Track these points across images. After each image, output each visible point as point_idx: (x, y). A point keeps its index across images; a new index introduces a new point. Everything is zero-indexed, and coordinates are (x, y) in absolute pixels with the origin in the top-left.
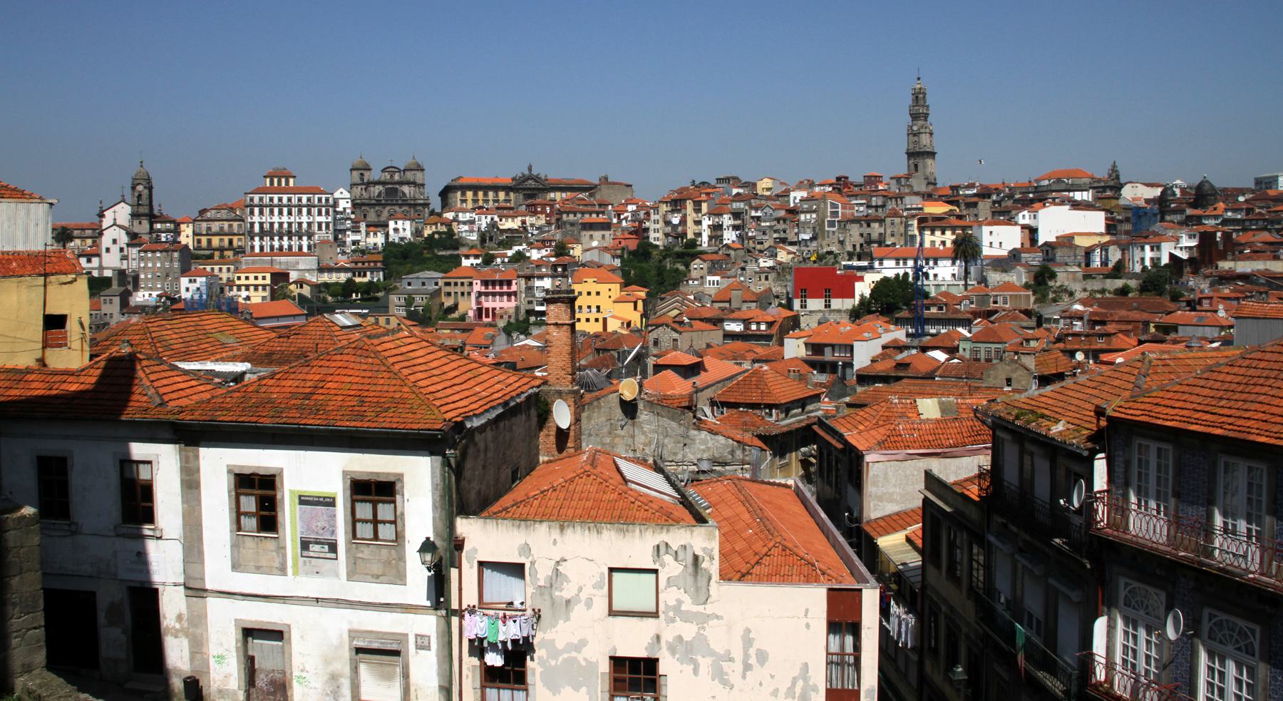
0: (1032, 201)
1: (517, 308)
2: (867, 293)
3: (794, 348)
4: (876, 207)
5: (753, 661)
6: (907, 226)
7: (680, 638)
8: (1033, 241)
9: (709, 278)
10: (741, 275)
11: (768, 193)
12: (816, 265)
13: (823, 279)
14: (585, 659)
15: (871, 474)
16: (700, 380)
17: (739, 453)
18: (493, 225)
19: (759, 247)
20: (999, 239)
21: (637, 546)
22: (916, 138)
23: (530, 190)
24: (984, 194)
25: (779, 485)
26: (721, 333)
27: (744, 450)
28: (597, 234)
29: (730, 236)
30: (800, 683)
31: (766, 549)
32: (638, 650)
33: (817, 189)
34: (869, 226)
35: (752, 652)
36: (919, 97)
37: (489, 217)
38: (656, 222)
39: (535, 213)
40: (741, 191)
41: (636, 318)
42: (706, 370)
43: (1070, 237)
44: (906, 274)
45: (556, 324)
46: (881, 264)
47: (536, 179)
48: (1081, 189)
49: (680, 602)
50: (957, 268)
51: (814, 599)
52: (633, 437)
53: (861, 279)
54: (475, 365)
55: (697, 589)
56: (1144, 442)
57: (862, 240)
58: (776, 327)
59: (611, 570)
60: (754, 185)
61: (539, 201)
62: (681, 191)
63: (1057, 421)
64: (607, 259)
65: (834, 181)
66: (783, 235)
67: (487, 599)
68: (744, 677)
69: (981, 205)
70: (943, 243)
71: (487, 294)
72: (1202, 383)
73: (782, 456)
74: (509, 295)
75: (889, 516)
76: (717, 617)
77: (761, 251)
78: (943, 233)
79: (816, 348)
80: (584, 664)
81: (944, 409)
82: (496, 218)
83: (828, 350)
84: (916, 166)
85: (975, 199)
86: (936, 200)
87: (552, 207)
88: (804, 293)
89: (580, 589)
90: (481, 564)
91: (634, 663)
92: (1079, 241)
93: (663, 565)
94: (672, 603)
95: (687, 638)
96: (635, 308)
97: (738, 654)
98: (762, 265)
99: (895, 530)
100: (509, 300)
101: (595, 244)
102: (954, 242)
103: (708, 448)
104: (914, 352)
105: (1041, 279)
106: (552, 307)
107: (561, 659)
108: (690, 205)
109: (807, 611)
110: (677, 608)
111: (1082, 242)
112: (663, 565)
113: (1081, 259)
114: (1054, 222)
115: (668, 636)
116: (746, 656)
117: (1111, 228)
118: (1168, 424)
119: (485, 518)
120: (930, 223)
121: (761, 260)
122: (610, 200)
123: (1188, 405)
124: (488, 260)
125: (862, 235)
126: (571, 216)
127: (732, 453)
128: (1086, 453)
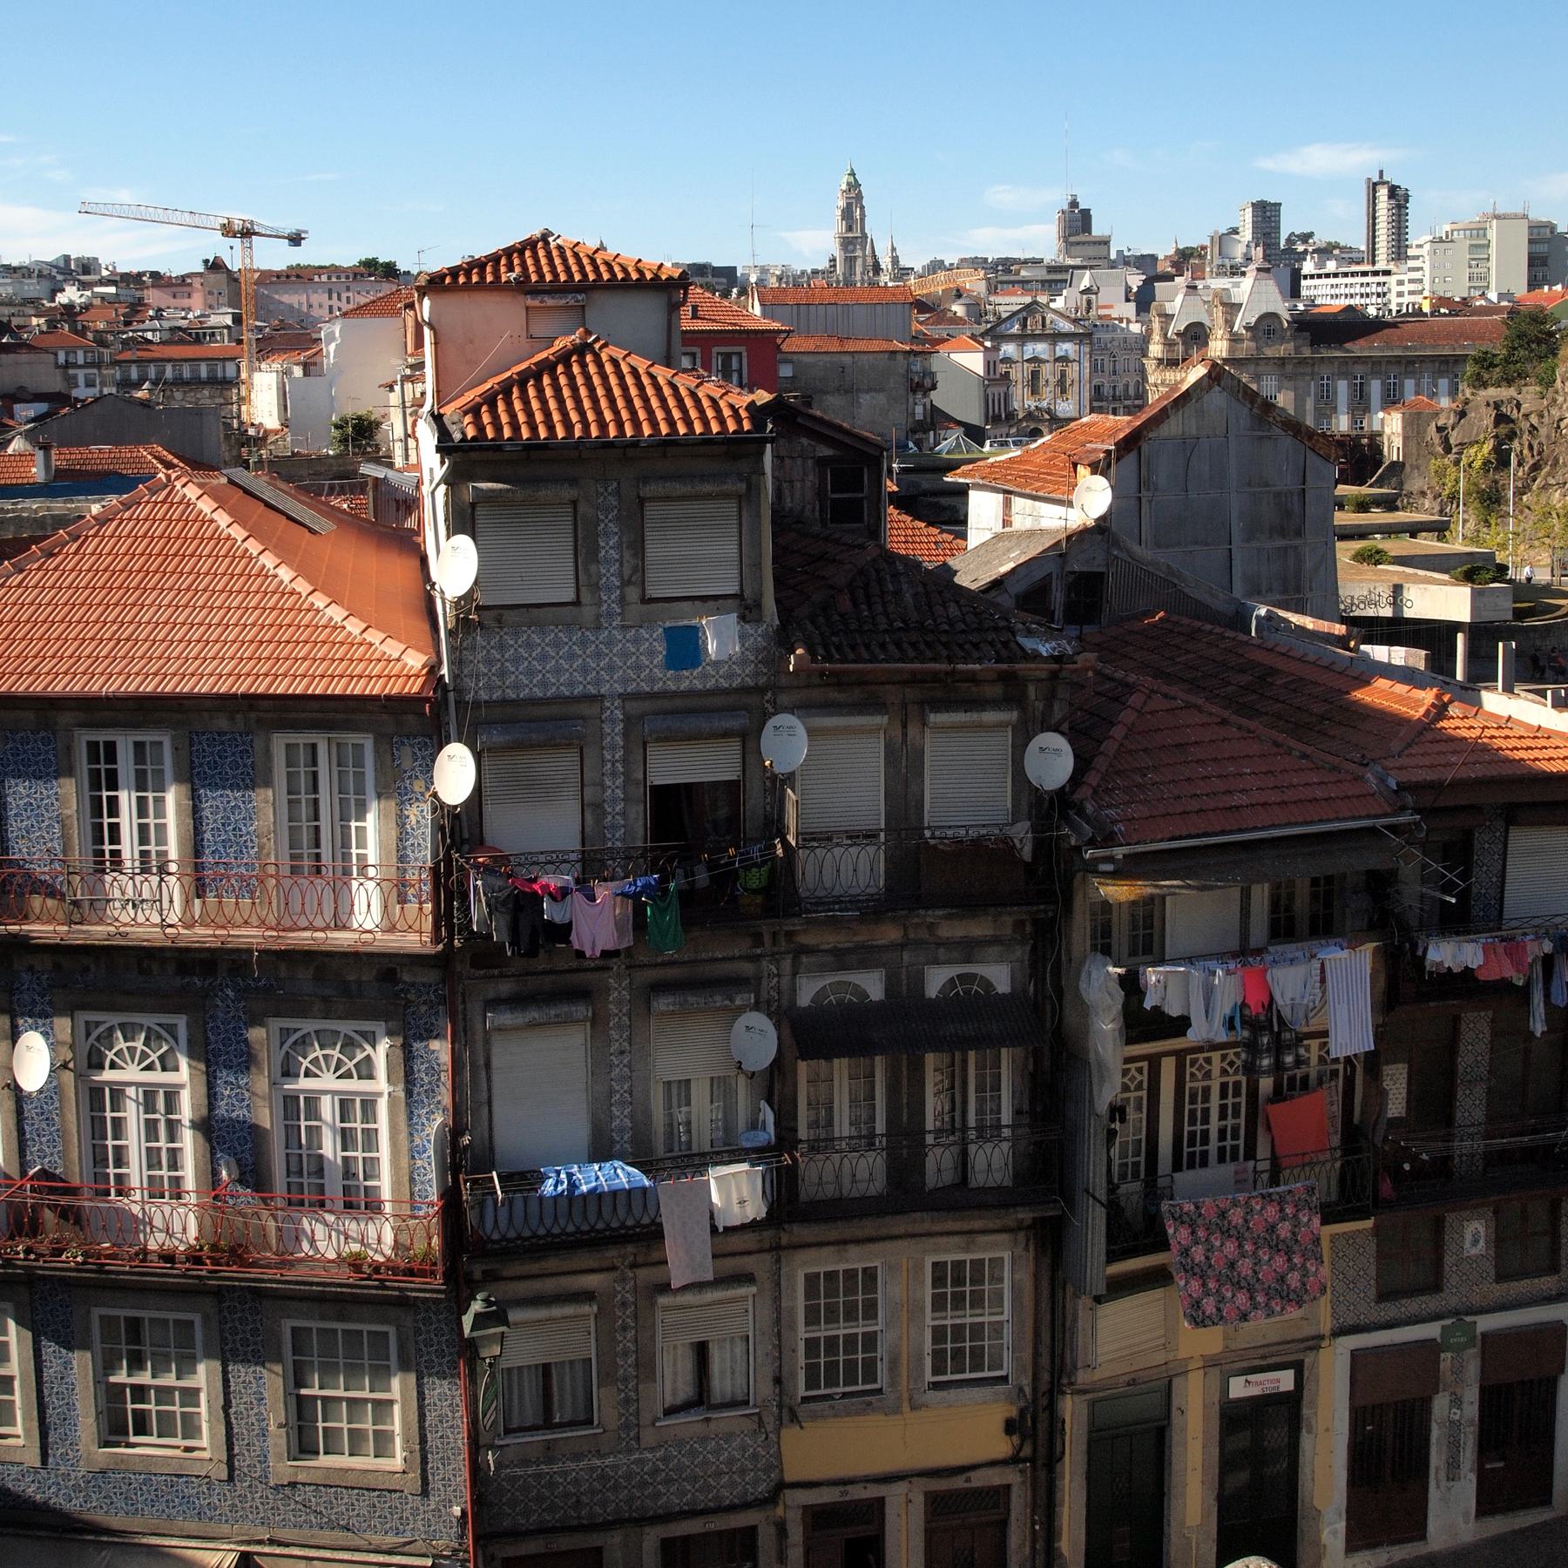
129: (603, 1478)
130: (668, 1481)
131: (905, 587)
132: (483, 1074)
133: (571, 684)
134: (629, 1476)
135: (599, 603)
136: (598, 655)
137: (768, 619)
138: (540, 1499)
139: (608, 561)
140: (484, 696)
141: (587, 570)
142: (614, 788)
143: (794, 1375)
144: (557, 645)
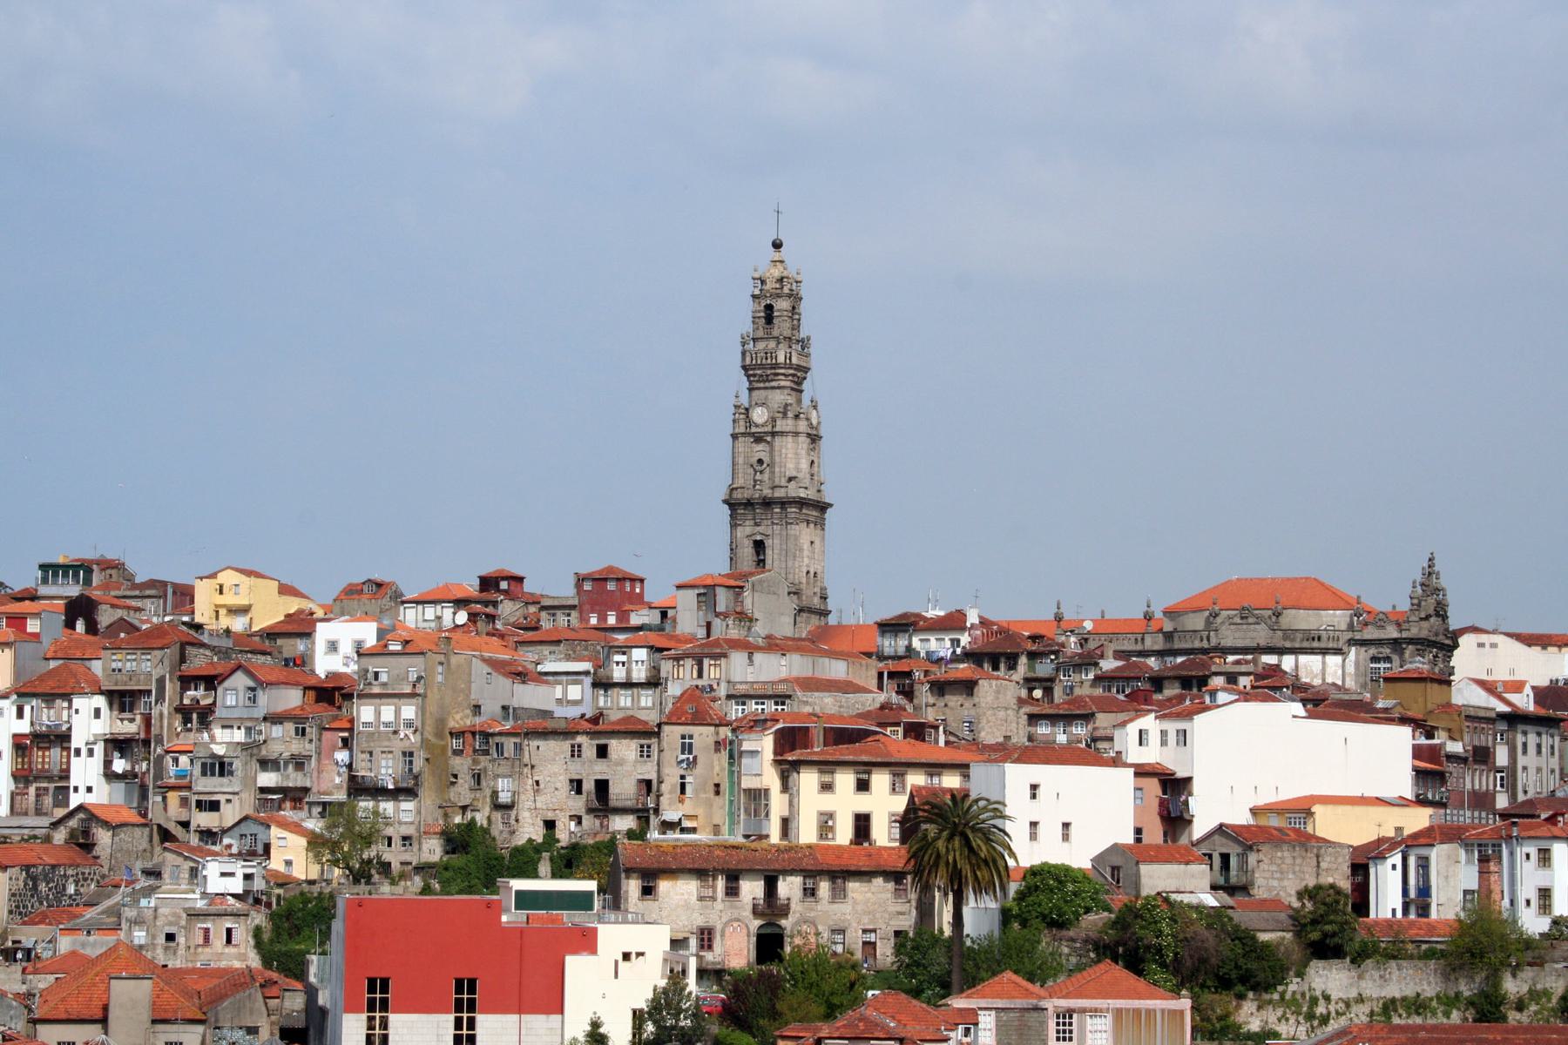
0: (1158, 682)
4: (628, 685)
6: (735, 756)
19: (204, 820)
22: (760, 451)
33: (411, 617)
34: (602, 752)
36: (775, 308)
43: (1303, 809)
48: (1314, 644)
53: (586, 942)
65: (471, 587)
66: (294, 779)
69: (987, 690)
77: (208, 835)
78: (863, 786)
84: (759, 546)
92: (1326, 824)
98: (216, 884)
102: (908, 824)
111: (1345, 829)
114: (1245, 757)
117: (1431, 773)
120: (818, 749)
121: (212, 869)
125: (577, 785)
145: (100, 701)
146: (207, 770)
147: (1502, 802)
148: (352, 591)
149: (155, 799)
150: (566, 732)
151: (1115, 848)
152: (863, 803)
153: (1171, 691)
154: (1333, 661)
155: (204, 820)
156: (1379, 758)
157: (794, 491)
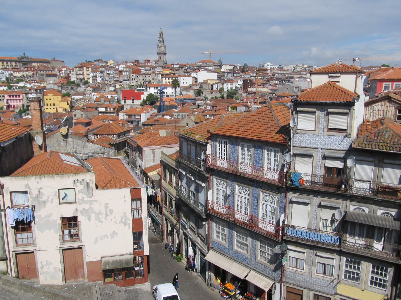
0: (196, 69)
1: (23, 105)
2: (145, 98)
3: (122, 116)
5: (108, 213)
6: (158, 76)
7: (84, 209)
8: (196, 82)
9: (93, 94)
10: (104, 93)
11: (112, 65)
12: (129, 89)
13: (131, 94)
14: (52, 220)
15: (145, 154)
16: (91, 127)
17: (102, 150)
18: (11, 74)
19: (110, 83)
20: (185, 81)
21: (67, 181)
22: (160, 48)
23: (25, 62)
24: (182, 67)
25: (116, 159)
26: (97, 112)
27: (105, 149)
28: (52, 78)
29: (99, 79)
30: (124, 219)
31: (111, 179)
32: (70, 214)
33: (128, 64)
34: (145, 76)
35: (108, 210)
37: (9, 72)
38: (73, 74)
39: (28, 71)
40: (103, 64)
41: (68, 107)
42: (92, 124)
43: (207, 80)
44: (157, 93)
45: (34, 109)
46: (149, 89)
47: (27, 58)
49: (83, 198)
50: (173, 90)
51: (126, 192)
52: (66, 146)
53: (143, 93)
54: (4, 124)
55: (89, 193)
56: (221, 140)
57: (143, 81)
58: (116, 109)
59: (59, 189)
60: (107, 63)
61: (29, 66)
62: (82, 64)
63: (197, 135)
64: (56, 87)
65: (134, 62)
67: (14, 204)
68: (106, 219)
70: (169, 82)
71: (11, 100)
72: (236, 122)
73: (118, 151)
74: (20, 100)
75: (152, 166)
76: (96, 201)
77: (110, 85)
78: (169, 79)
79: (130, 116)
80: (52, 221)
81: (167, 134)
82: (12, 72)
83: (133, 117)
84: (160, 57)
85: (179, 68)
86: (166, 69)
87: (34, 68)
88: (125, 98)
89: (48, 197)
90: (11, 192)
91: (69, 219)
92: (210, 82)
93: (77, 186)
94: (80, 198)
95: (86, 208)
96: (68, 104)
97: (103, 211)
99: (153, 171)
100: (20, 102)
101: (51, 82)
102: (172, 82)
103: (92, 149)
104: (160, 116)
105: (199, 93)
106: (32, 103)
107: (43, 221)
108: (85, 68)
109: (124, 196)
110: (82, 199)
112: (77, 186)
113: (210, 87)
114: (202, 76)
115: (80, 208)
116: (106, 212)
117: (219, 77)
118: (227, 134)
119: (11, 177)
122: (55, 66)
123: (233, 129)
124: (10, 87)
125: (143, 80)
126: (42, 72)
127: (101, 150)
128: (205, 144)
129: (305, 280)
130: (316, 285)
131: (387, 134)
132: (291, 208)
133: (313, 144)
134: (309, 281)
135: (319, 131)
136: (318, 140)
137: (352, 137)
138: (293, 279)
139: (321, 123)
140: (297, 145)
141: (317, 125)
142: (319, 164)
143: (341, 275)
144: (311, 138)
145: (99, 73)
146: (110, 79)
147: (225, 79)
148: (123, 62)
149: (105, 81)
150: (142, 75)
151: (190, 84)
152: (169, 81)
153: (197, 70)
154: (212, 67)
155: (110, 83)
156: (214, 76)
157: (163, 52)
